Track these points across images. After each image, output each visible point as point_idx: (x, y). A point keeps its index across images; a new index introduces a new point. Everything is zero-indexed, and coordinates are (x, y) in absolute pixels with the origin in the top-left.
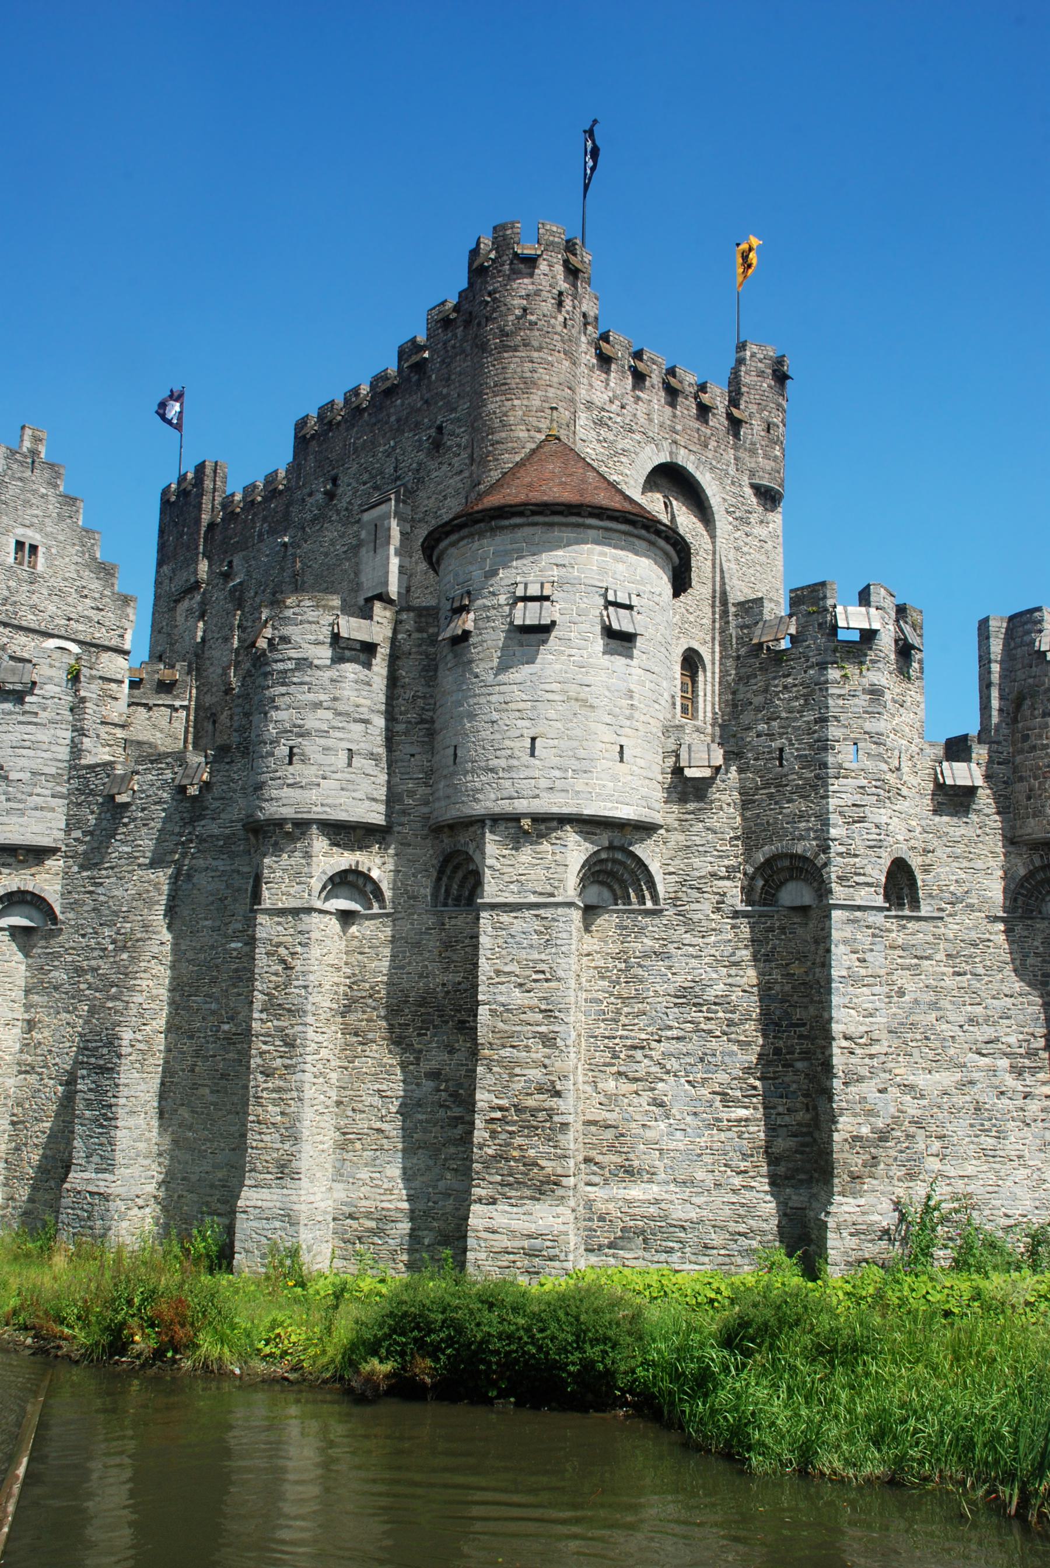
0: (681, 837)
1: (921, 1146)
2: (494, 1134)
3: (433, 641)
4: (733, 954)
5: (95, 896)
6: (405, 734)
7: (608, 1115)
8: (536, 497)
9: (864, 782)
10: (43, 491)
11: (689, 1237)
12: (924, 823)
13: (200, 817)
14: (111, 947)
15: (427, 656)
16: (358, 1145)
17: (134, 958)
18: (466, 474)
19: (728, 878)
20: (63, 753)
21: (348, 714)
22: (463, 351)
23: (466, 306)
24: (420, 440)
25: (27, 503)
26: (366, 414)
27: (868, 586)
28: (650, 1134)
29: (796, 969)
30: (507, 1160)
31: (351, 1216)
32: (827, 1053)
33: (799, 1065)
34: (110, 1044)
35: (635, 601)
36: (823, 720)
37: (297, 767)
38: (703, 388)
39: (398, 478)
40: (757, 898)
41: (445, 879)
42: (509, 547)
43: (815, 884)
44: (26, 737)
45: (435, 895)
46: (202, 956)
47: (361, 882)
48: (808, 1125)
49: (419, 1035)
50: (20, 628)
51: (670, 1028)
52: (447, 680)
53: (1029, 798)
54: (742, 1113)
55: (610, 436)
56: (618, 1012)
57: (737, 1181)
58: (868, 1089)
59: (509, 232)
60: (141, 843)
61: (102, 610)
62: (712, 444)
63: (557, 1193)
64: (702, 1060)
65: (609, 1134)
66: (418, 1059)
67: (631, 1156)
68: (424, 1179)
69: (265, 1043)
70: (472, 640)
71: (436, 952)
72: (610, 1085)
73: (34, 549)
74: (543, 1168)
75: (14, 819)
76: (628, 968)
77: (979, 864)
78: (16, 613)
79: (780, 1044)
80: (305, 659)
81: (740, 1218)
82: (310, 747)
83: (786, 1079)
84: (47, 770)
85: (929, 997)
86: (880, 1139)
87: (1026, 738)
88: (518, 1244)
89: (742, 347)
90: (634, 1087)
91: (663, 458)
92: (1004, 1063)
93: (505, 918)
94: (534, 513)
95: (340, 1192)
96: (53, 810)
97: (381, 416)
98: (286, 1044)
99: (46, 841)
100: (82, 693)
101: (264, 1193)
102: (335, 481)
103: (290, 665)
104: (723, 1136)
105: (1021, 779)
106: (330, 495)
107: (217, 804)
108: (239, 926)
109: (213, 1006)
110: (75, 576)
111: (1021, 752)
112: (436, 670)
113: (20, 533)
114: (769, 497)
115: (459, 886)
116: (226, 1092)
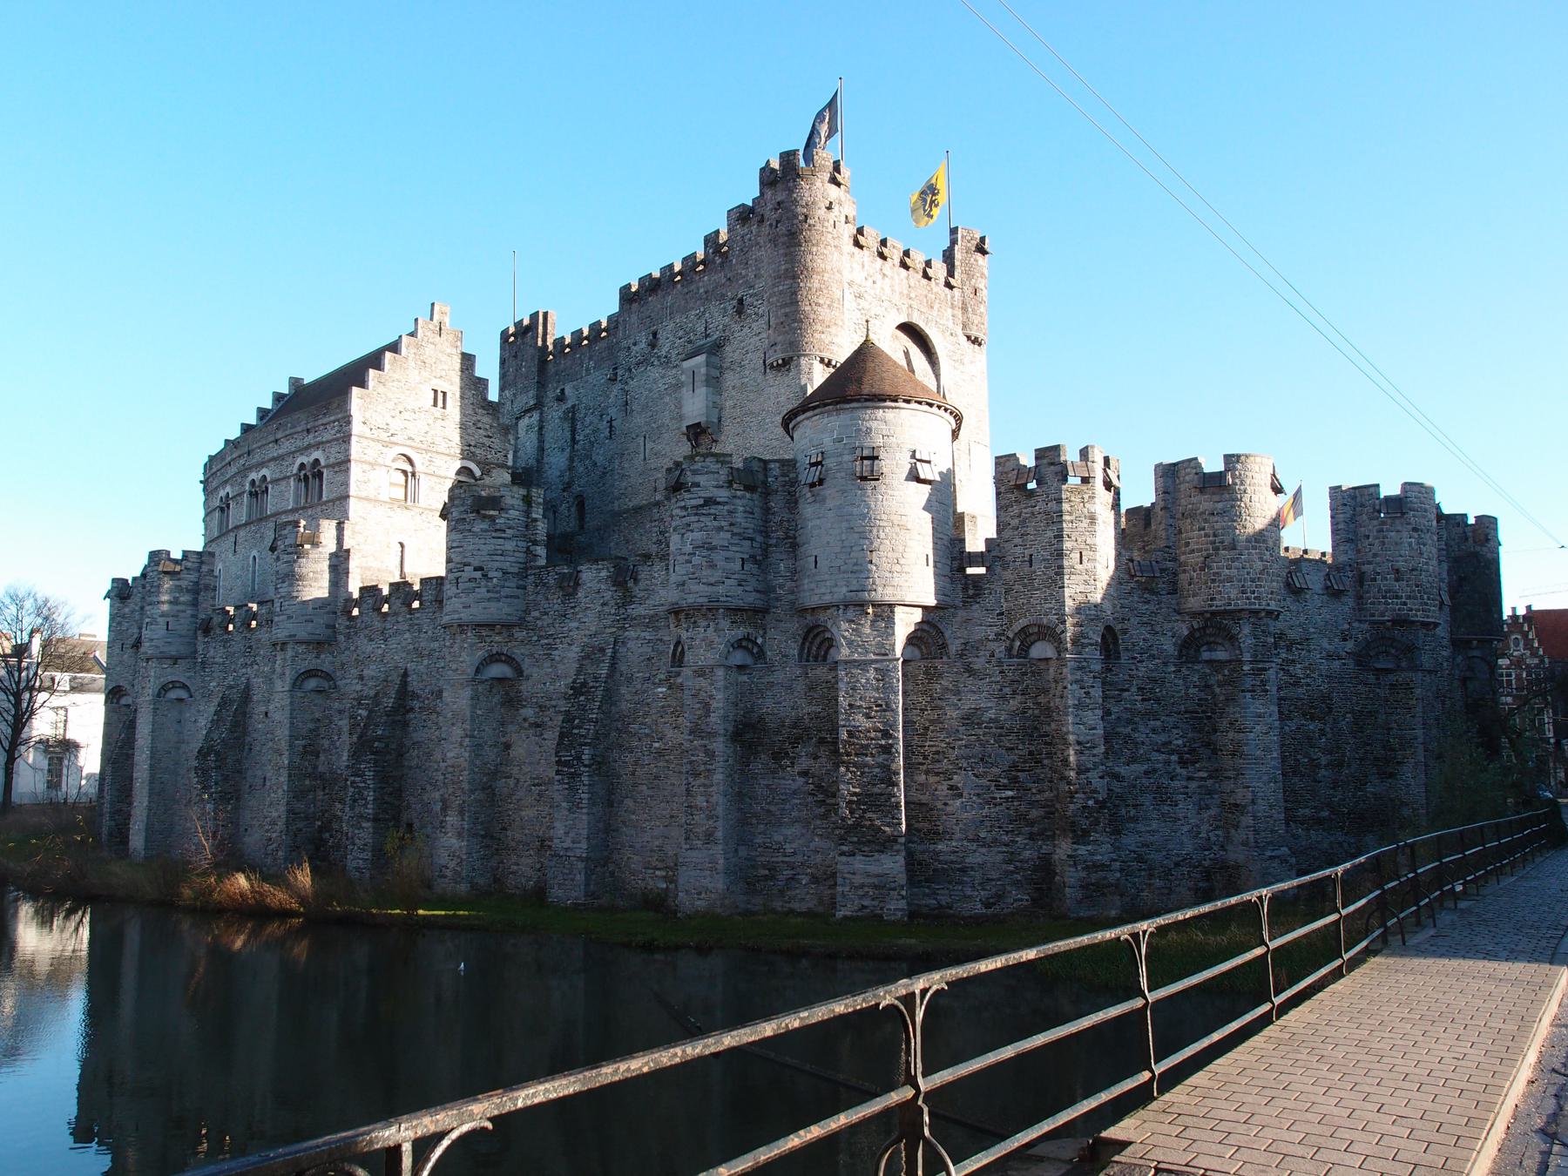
0: (965, 614)
1: (1123, 812)
3: (794, 482)
4: (1001, 690)
6: (776, 546)
7: (922, 797)
8: (866, 389)
9: (1087, 577)
12: (1122, 601)
13: (632, 602)
15: (789, 493)
17: (588, 699)
18: (764, 335)
19: (994, 640)
20: (521, 556)
21: (739, 534)
22: (758, 244)
23: (758, 210)
24: (724, 308)
26: (679, 286)
27: (1087, 447)
28: (949, 809)
29: (1042, 699)
30: (862, 827)
31: (753, 867)
32: (1066, 754)
33: (1046, 762)
34: (579, 758)
35: (932, 458)
36: (1059, 537)
37: (709, 572)
38: (928, 264)
39: (707, 336)
40: (1015, 652)
41: (807, 644)
42: (850, 423)
43: (1056, 644)
44: (498, 547)
45: (800, 655)
46: (637, 698)
47: (750, 646)
48: (1052, 801)
49: (793, 748)
51: (962, 740)
52: (807, 510)
53: (1190, 584)
54: (1010, 793)
55: (867, 307)
56: (926, 729)
57: (1006, 838)
59: (791, 158)
60: (586, 620)
62: (936, 306)
63: (895, 848)
64: (982, 760)
65: (924, 809)
66: (793, 763)
67: (938, 823)
68: (800, 842)
69: (693, 755)
70: (825, 486)
71: (802, 692)
74: (885, 832)
75: (493, 604)
76: (933, 699)
77: (1158, 628)
79: (1033, 748)
80: (711, 498)
81: (1010, 862)
82: (718, 557)
87: (1187, 544)
89: (954, 231)
90: (938, 779)
91: (903, 319)
92: (1174, 758)
94: (866, 400)
95: (743, 852)
96: (518, 597)
97: (693, 287)
99: (514, 619)
100: (534, 516)
101: (694, 853)
102: (655, 334)
103: (702, 502)
105: (1184, 571)
106: (653, 345)
107: (642, 594)
108: (663, 677)
109: (646, 731)
110: (472, 413)
111: (1184, 553)
112: (796, 502)
114: (976, 341)
115: (819, 648)
116: (659, 788)
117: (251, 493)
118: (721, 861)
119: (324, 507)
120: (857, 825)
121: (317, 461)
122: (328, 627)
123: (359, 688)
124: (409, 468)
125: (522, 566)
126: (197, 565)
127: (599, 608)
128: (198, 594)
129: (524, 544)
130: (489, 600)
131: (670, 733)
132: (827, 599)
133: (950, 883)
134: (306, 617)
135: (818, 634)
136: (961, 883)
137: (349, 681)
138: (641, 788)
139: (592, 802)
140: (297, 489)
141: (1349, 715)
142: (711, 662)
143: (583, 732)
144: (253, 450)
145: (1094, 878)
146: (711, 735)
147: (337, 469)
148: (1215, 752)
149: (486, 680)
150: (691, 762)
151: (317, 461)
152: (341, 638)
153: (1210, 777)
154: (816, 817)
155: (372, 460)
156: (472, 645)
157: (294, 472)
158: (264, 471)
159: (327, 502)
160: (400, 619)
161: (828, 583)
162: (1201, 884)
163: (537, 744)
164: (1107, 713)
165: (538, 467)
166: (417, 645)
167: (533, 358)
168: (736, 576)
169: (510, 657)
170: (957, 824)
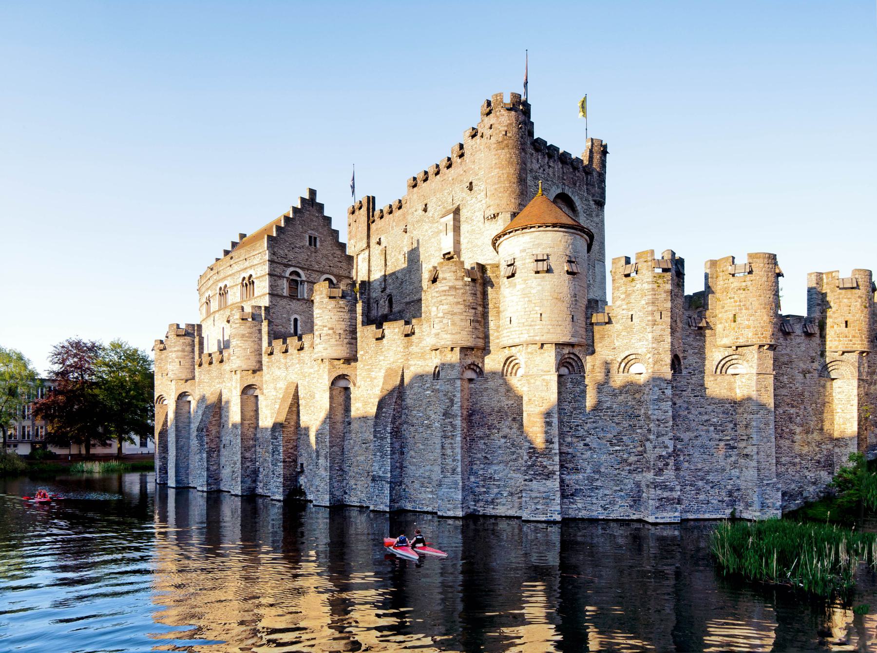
1: (682, 458)
2: (530, 458)
11: (601, 492)
16: (478, 462)
31: (478, 486)
41: (506, 366)
47: (475, 368)
50: (314, 270)
54: (618, 448)
56: (572, 412)
57: (616, 472)
58: (666, 439)
65: (569, 456)
72: (569, 439)
73: (315, 238)
79: (631, 423)
81: (617, 485)
83: (634, 436)
85: (685, 405)
86: (669, 456)
88: (541, 495)
92: (712, 428)
93: (532, 381)
95: (472, 479)
98: (452, 427)
101: (446, 480)
104: (611, 456)
108: (428, 385)
109: (421, 415)
115: (512, 369)
117: (220, 294)
118: (461, 484)
120: (532, 465)
124: (299, 279)
127: (395, 349)
131: (433, 416)
132: (517, 341)
133: (584, 496)
135: (512, 361)
136: (590, 497)
138: (418, 445)
139: (393, 453)
141: (814, 405)
142: (454, 377)
143: (387, 415)
145: (666, 494)
146: (454, 416)
147: (261, 279)
148: (735, 425)
150: (444, 431)
151: (251, 276)
152: (264, 368)
153: (732, 439)
154: (511, 460)
156: (329, 370)
161: (517, 333)
162: (725, 499)
164: (675, 404)
168: (467, 329)
170: (588, 465)
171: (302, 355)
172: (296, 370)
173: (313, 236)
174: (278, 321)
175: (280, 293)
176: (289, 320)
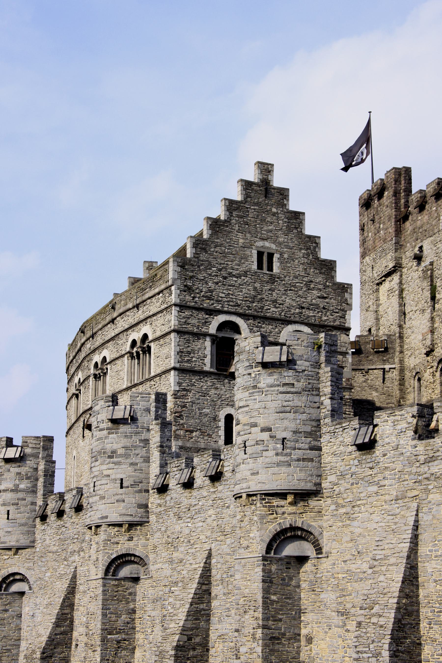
5: (351, 529)
10: (274, 210)
14: (370, 571)
25: (263, 220)
50: (265, 318)
61: (325, 298)
73: (271, 256)
75: (284, 469)
78: (262, 308)
84: (303, 428)
96: (312, 460)
99: (309, 486)
110: (303, 274)
113: (260, 244)
117: (95, 376)
119: (152, 383)
121: (145, 336)
122: (140, 506)
123: (168, 572)
125: (314, 424)
126: (35, 451)
128: (37, 480)
129: (316, 399)
130: (278, 464)
134: (117, 497)
137: (159, 566)
140: (131, 367)
143: (382, 621)
144: (96, 333)
149: (281, 559)
151: (145, 336)
152: (152, 518)
155: (195, 330)
156: (262, 517)
157: (128, 349)
158: (105, 353)
159: (155, 376)
160: (205, 493)
163: (340, 636)
165: (400, 333)
166: (220, 522)
167: (389, 220)
169: (307, 531)
171: (220, 488)
172: (209, 520)
173: (266, 251)
174: (192, 422)
175: (196, 365)
176: (215, 419)
